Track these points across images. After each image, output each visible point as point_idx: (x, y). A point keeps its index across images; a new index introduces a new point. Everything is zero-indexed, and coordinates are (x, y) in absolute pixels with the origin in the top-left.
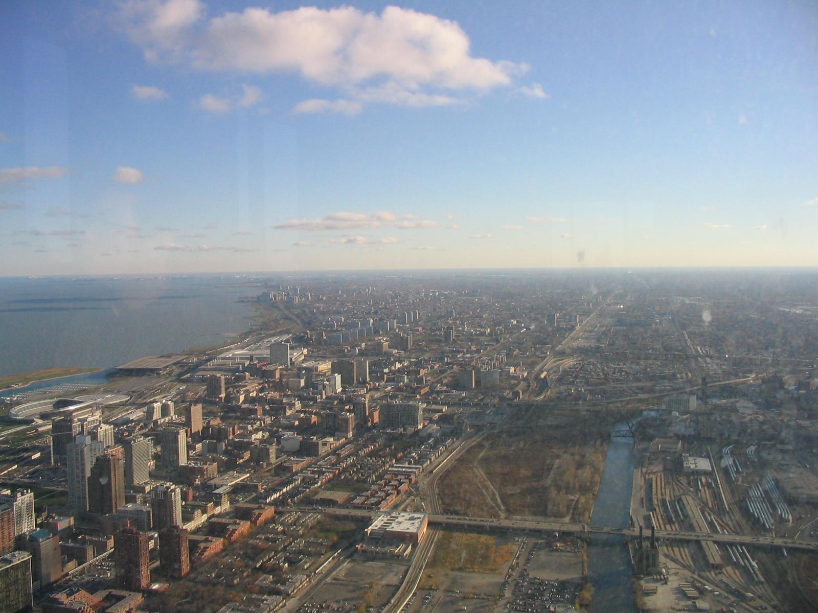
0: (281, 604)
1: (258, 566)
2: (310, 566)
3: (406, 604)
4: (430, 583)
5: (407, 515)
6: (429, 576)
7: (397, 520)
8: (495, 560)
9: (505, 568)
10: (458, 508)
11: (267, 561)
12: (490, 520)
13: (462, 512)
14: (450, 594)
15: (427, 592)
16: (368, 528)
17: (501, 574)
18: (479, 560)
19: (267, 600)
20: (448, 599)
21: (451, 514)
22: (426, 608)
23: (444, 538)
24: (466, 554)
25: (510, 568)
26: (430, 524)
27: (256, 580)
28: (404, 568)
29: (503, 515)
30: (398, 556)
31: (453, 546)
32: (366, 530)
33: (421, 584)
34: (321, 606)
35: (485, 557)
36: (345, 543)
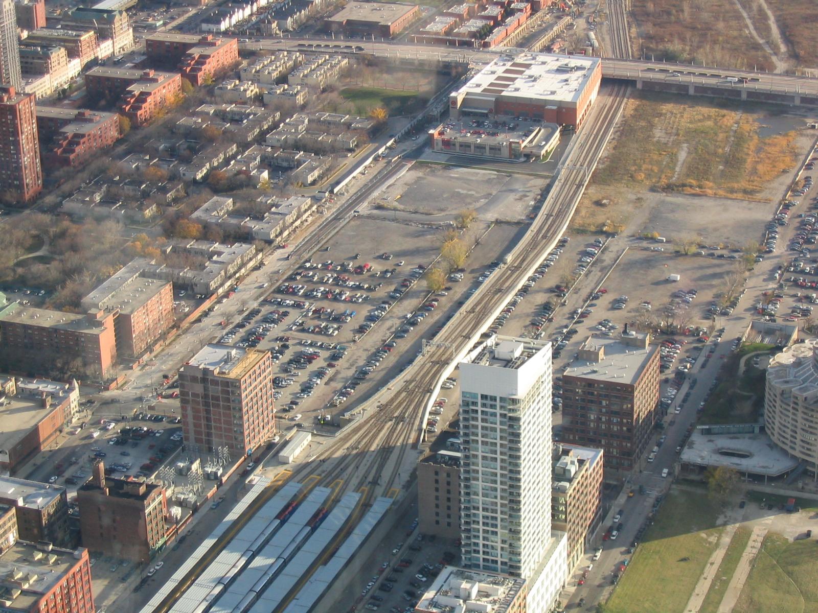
0: (251, 264)
1: (199, 176)
2: (321, 177)
3: (543, 266)
4: (600, 219)
5: (552, 61)
6: (598, 203)
7: (528, 72)
8: (754, 171)
9: (777, 189)
10: (675, 46)
11: (221, 166)
12: (750, 76)
13: (685, 56)
14: (645, 244)
15: (592, 240)
16: (457, 89)
17: (767, 201)
18: (719, 168)
19: (219, 254)
20: (639, 255)
21: (659, 59)
22: (587, 275)
23: (638, 115)
24: (689, 153)
25: (789, 188)
26: (608, 82)
27: (196, 209)
28: (541, 183)
29: (781, 66)
30: (528, 156)
31: (658, 134)
32: (453, 94)
33: (579, 221)
34: (344, 269)
35: (733, 162)
36: (403, 125)
